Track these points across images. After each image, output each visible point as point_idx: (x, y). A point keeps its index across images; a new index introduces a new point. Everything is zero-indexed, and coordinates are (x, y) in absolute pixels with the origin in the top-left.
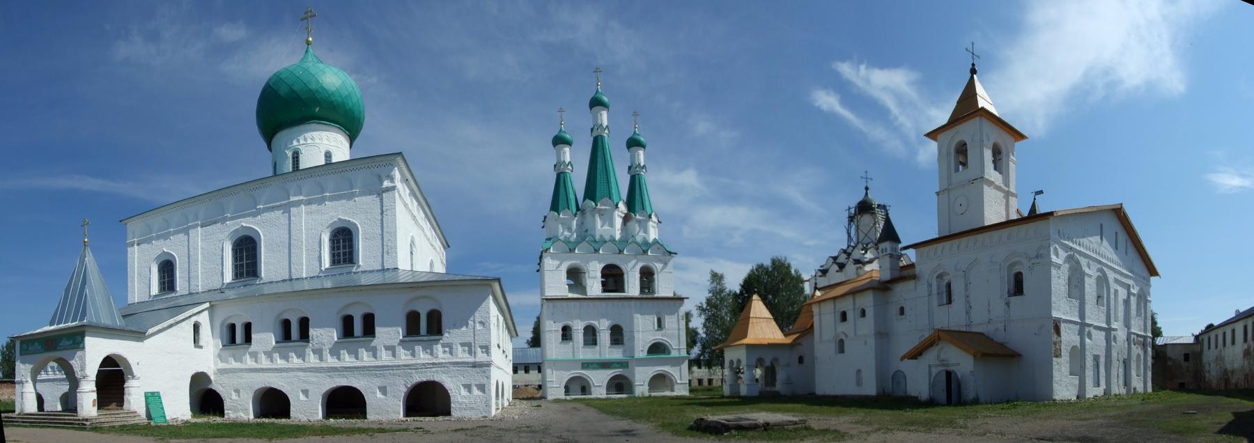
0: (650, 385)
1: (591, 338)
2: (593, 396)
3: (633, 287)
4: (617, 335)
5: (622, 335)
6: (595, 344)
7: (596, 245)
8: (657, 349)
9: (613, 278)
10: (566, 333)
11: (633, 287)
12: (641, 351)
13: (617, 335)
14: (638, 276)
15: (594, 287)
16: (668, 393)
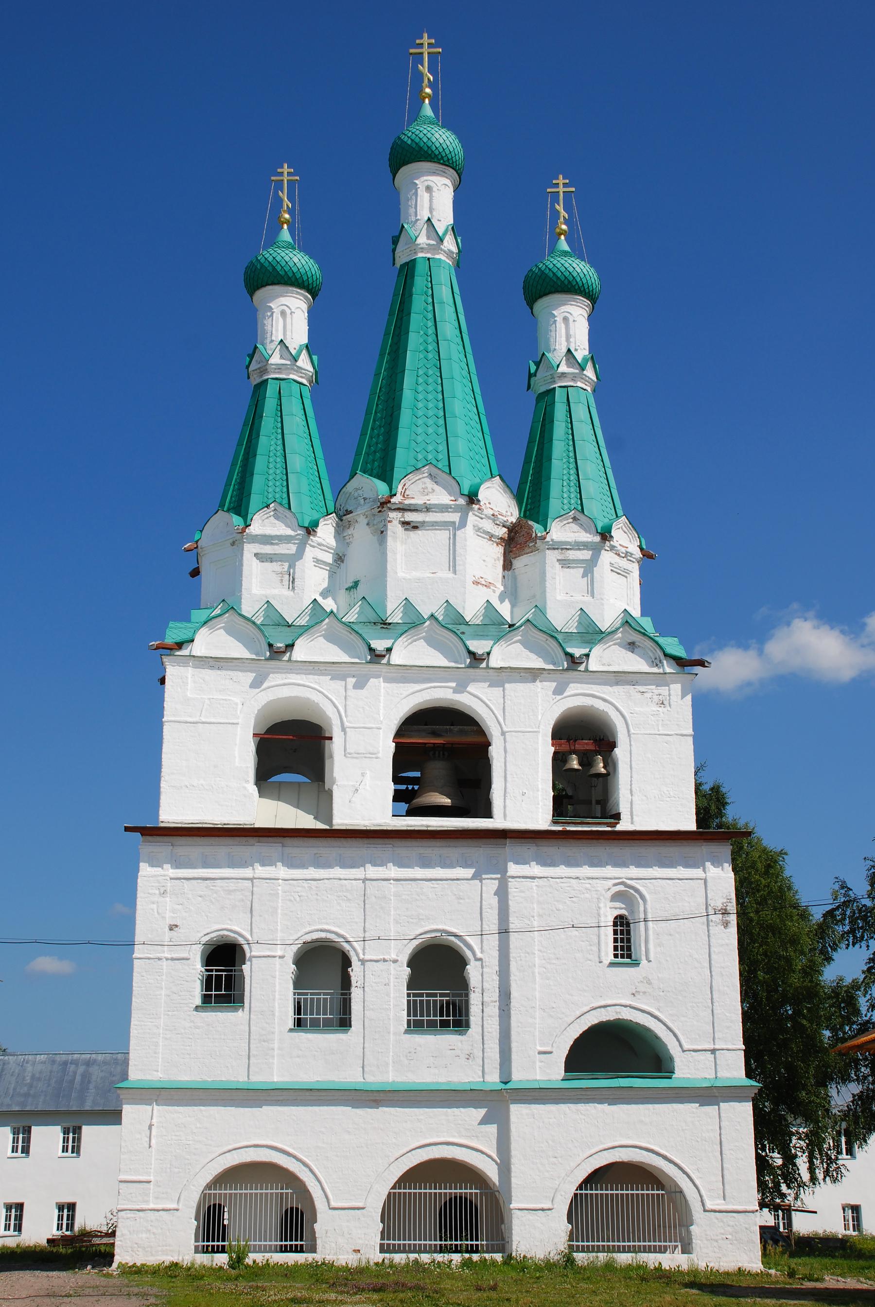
0: (577, 1209)
1: (325, 995)
2: (318, 1257)
3: (523, 791)
4: (439, 980)
5: (462, 985)
6: (344, 1023)
7: (371, 634)
8: (614, 1053)
9: (443, 758)
10: (223, 969)
11: (523, 791)
12: (542, 1058)
13: (439, 980)
14: (546, 750)
15: (362, 788)
16: (672, 1260)
